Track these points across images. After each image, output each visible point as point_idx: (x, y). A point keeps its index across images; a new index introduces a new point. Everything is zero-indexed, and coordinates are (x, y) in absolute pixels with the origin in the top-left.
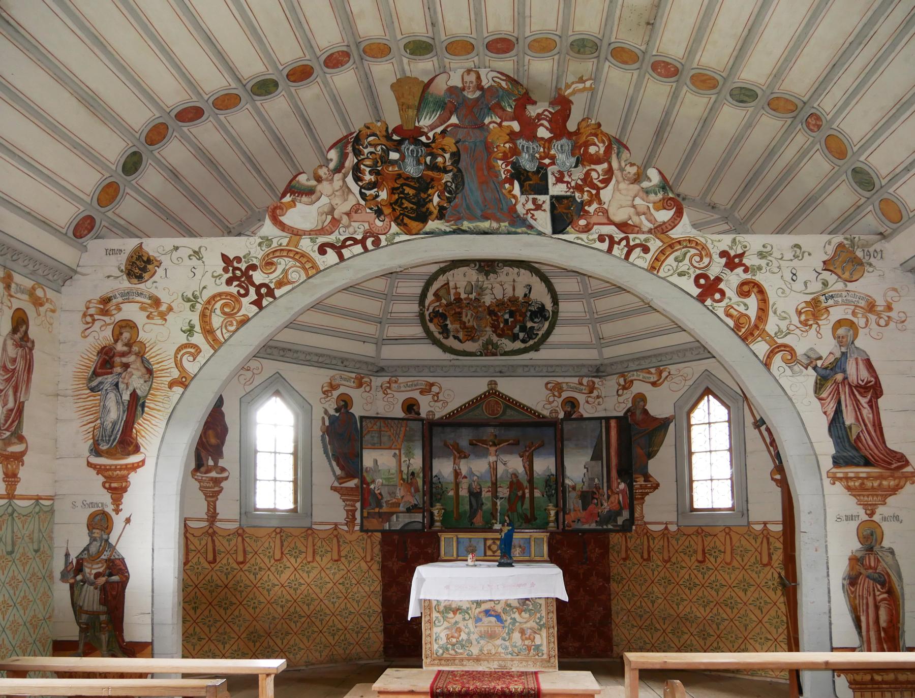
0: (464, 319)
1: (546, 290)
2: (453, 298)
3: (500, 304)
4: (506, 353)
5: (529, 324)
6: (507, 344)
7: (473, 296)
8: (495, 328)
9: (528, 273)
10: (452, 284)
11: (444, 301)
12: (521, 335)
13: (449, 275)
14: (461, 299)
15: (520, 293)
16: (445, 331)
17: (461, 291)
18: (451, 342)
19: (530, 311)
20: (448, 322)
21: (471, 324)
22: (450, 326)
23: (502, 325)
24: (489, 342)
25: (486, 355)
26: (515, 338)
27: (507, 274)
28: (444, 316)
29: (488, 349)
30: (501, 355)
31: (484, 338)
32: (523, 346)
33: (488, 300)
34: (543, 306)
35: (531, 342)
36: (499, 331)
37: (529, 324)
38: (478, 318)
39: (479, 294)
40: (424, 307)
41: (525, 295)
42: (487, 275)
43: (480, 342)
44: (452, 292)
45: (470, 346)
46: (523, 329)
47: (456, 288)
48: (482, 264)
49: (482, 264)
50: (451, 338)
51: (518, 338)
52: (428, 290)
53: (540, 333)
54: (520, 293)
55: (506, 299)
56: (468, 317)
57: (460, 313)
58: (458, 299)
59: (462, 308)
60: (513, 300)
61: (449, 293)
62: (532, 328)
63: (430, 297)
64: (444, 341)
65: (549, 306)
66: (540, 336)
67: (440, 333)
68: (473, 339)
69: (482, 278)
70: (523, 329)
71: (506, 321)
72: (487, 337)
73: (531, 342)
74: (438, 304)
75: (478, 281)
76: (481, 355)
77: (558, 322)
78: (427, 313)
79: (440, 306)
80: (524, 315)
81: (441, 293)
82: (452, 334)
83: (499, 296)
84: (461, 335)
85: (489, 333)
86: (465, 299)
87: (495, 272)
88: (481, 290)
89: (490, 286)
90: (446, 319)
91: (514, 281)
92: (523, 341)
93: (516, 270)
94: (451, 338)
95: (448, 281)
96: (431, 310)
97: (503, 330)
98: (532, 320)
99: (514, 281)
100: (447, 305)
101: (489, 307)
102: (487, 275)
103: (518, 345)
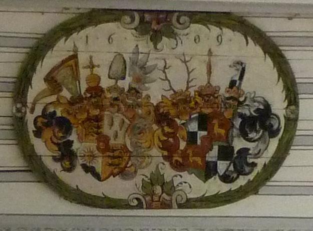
0: (106, 130)
1: (275, 73)
2: (84, 86)
3: (181, 101)
4: (189, 204)
5: (239, 144)
6: (193, 185)
7: (125, 84)
8: (169, 150)
9: (238, 37)
10: (83, 59)
11: (66, 94)
12: (222, 166)
13: (78, 37)
14: (102, 90)
15: (221, 79)
16: (66, 155)
17: (102, 72)
18: (79, 179)
19: (241, 116)
20: (73, 137)
21: (120, 141)
22: (76, 146)
23: (183, 145)
24: (156, 179)
25: (149, 207)
26: (208, 171)
27: (197, 39)
28: (64, 125)
29: (153, 194)
30: (181, 206)
31: (146, 172)
32: (225, 188)
33: (156, 92)
34: (267, 107)
35: (242, 181)
36: (177, 158)
37: (239, 144)
38: (134, 130)
39: (138, 80)
40: (24, 104)
41: (233, 84)
42: (155, 38)
43: (138, 179)
44: (84, 73)
45: (117, 188)
46: (226, 153)
47: (92, 66)
48: (147, 17)
49: (147, 17)
50: (79, 170)
51: (215, 171)
52: (34, 69)
53: (261, 162)
54: (221, 79)
55: (192, 92)
56: (114, 127)
57: (98, 119)
58: (96, 91)
59: (102, 108)
60: (208, 94)
61: (76, 77)
62: (244, 152)
63: (38, 84)
64: (64, 176)
65: (279, 106)
66: (259, 169)
67: (55, 159)
68: (123, 173)
69: (145, 45)
70: (226, 153)
71: (192, 136)
72: (152, 168)
73: (242, 181)
74: (53, 98)
75: (136, 52)
76: (140, 206)
77: (296, 140)
78: (30, 118)
79: (58, 103)
80: (227, 125)
81: (59, 78)
82: (81, 161)
83: (180, 86)
84: (99, 165)
85: (156, 161)
86: (110, 89)
87: (172, 35)
88: (143, 72)
89: (161, 64)
90: (68, 131)
91: (210, 53)
92: (226, 179)
93: (215, 30)
94: (79, 170)
95: (76, 50)
96: (38, 111)
97: (184, 155)
98: (244, 135)
99: (210, 53)
100: (72, 103)
101: (157, 108)
102: (155, 38)
103: (215, 186)
